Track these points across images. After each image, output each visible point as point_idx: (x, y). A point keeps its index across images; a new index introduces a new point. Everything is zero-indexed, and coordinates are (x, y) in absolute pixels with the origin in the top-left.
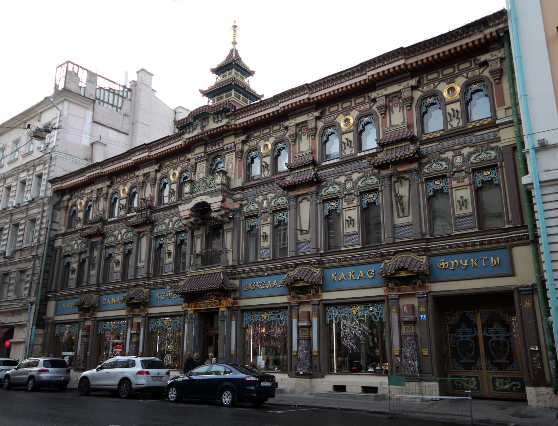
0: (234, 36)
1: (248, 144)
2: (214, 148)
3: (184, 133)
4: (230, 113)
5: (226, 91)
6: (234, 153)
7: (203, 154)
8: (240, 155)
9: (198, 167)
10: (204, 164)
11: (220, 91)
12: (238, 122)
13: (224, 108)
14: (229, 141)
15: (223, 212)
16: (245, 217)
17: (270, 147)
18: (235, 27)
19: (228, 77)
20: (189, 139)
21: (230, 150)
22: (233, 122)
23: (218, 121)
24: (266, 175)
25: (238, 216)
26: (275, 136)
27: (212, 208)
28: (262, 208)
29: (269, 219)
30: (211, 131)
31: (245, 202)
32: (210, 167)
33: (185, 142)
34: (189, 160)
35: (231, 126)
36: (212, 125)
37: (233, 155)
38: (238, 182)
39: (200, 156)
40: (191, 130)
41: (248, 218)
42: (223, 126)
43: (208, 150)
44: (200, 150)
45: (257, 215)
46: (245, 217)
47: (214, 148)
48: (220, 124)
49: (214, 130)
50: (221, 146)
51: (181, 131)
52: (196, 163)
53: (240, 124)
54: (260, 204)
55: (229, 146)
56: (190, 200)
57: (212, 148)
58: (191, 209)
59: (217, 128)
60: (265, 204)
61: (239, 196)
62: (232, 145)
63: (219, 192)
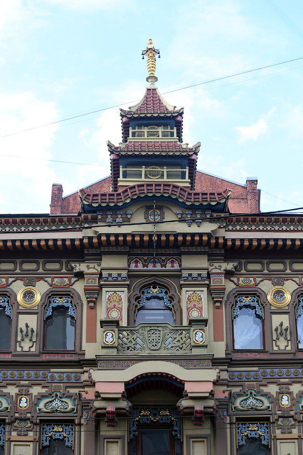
0: (152, 68)
1: (235, 280)
2: (151, 267)
3: (95, 220)
4: (222, 215)
5: (169, 165)
6: (205, 289)
7: (124, 273)
8: (215, 294)
9: (106, 294)
10: (124, 294)
11: (155, 160)
12: (231, 235)
13: (219, 203)
14: (196, 264)
15: (211, 403)
16: (238, 419)
17: (288, 297)
18: (151, 52)
19: (160, 139)
20: (108, 236)
21: (194, 282)
22: (222, 233)
23: (194, 221)
24: (282, 347)
25: (225, 413)
26: (297, 280)
27: (188, 388)
28: (280, 409)
29: (295, 431)
30: (168, 236)
31: (237, 390)
32: (133, 301)
33: (90, 238)
34: (80, 275)
35: (217, 238)
36: (174, 225)
37: (204, 294)
38: (220, 350)
39: (115, 273)
40: (119, 220)
41: (244, 420)
42: (201, 235)
43: (133, 266)
44: (114, 264)
45: (268, 419)
46: (238, 419)
47: (151, 267)
48: (194, 229)
49: (176, 235)
50: (169, 266)
51: (89, 216)
52: (101, 286)
53: (234, 240)
54: (276, 401)
55: (195, 273)
56: (126, 363)
57: (154, 266)
58: (127, 384)
59: (185, 235)
60: (285, 401)
61: (225, 375)
62: (204, 273)
63: (206, 363)
